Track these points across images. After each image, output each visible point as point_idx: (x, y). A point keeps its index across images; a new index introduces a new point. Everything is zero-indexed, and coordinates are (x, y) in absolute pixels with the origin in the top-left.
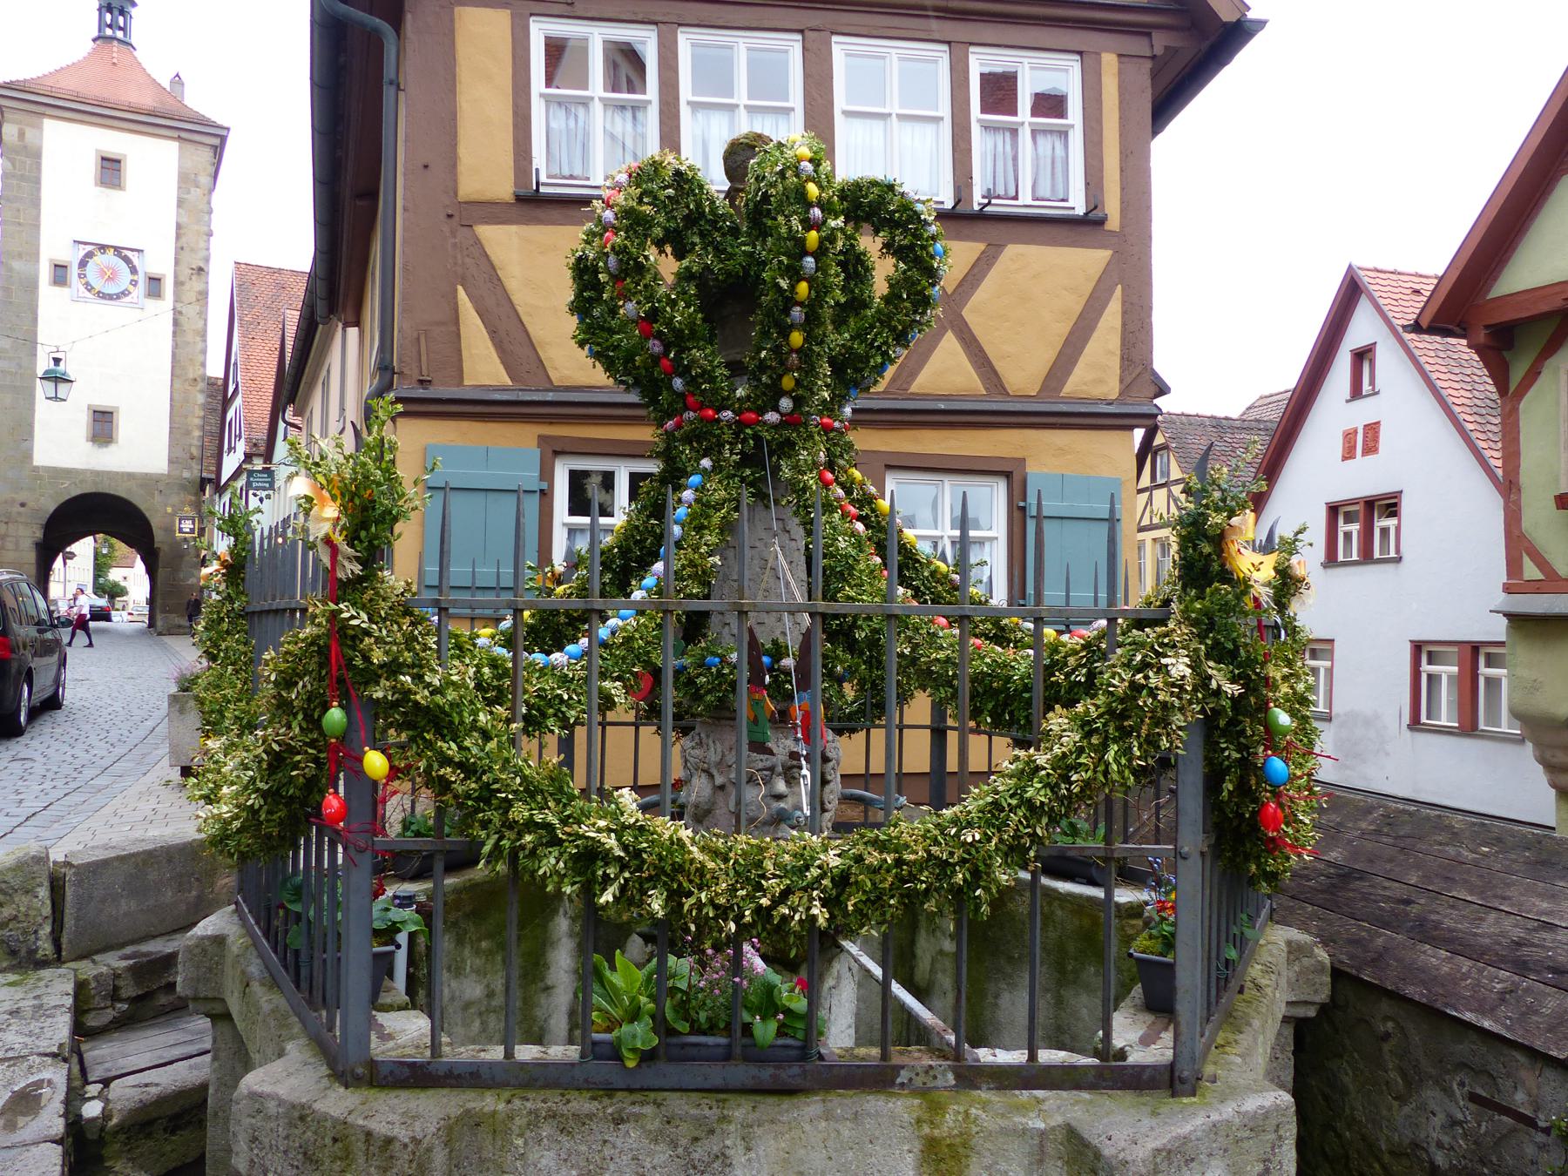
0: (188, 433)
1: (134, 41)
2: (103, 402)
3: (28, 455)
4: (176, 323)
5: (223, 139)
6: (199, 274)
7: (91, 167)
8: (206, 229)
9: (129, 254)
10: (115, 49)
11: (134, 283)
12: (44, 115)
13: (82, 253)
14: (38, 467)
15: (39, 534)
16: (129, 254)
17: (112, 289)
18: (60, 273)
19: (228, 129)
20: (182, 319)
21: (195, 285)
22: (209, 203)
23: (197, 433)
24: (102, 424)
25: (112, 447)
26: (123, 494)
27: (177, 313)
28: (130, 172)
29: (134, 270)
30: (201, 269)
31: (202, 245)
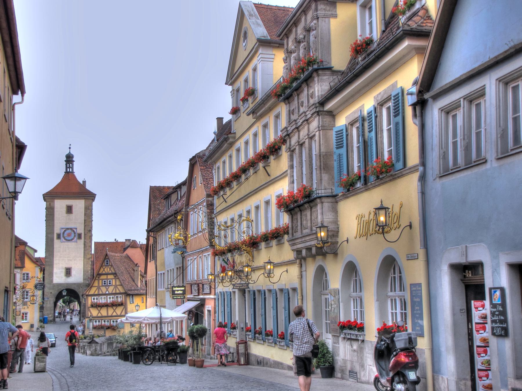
0: (88, 272)
1: (74, 171)
2: (68, 266)
3: (52, 281)
4: (84, 244)
5: (95, 197)
6: (90, 232)
7: (64, 209)
8: (91, 220)
9: (74, 229)
10: (70, 175)
11: (75, 236)
12: (55, 199)
13: (63, 231)
14: (54, 284)
15: (55, 300)
16: (74, 229)
17: (70, 238)
18: (59, 237)
19: (96, 195)
20: (86, 243)
21: (89, 235)
22: (92, 213)
23: (90, 272)
24: (68, 272)
25: (71, 277)
26: (73, 289)
27: (85, 242)
28: (74, 210)
29: (75, 233)
30: (90, 230)
31: (90, 224)
